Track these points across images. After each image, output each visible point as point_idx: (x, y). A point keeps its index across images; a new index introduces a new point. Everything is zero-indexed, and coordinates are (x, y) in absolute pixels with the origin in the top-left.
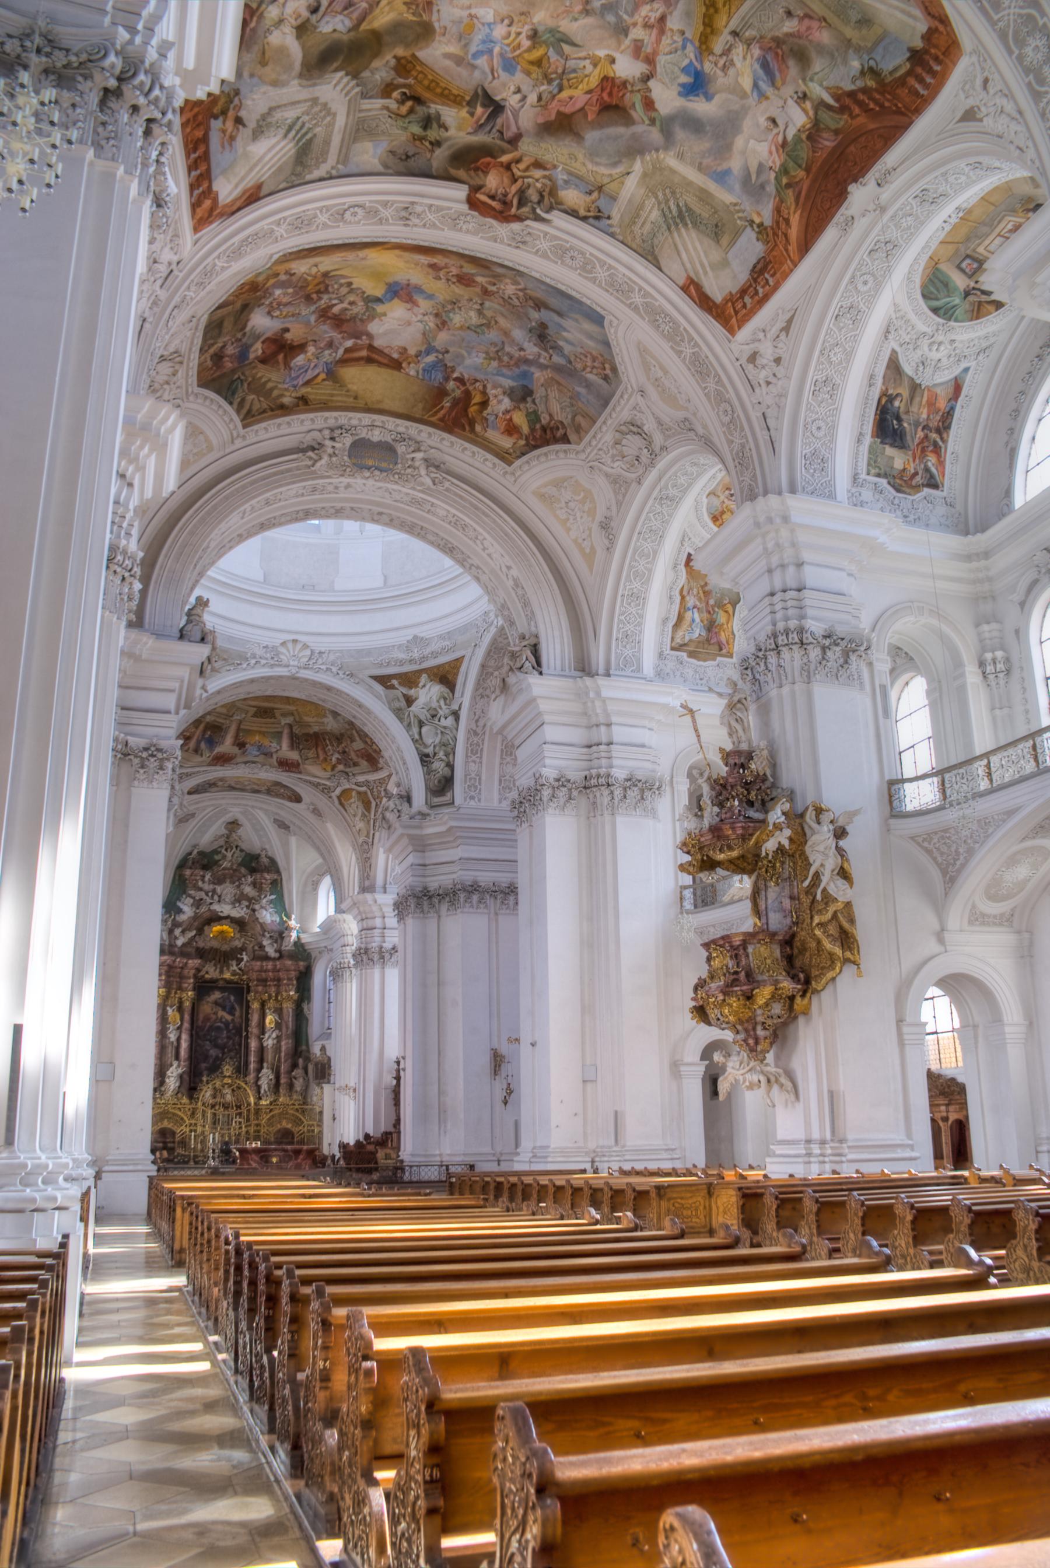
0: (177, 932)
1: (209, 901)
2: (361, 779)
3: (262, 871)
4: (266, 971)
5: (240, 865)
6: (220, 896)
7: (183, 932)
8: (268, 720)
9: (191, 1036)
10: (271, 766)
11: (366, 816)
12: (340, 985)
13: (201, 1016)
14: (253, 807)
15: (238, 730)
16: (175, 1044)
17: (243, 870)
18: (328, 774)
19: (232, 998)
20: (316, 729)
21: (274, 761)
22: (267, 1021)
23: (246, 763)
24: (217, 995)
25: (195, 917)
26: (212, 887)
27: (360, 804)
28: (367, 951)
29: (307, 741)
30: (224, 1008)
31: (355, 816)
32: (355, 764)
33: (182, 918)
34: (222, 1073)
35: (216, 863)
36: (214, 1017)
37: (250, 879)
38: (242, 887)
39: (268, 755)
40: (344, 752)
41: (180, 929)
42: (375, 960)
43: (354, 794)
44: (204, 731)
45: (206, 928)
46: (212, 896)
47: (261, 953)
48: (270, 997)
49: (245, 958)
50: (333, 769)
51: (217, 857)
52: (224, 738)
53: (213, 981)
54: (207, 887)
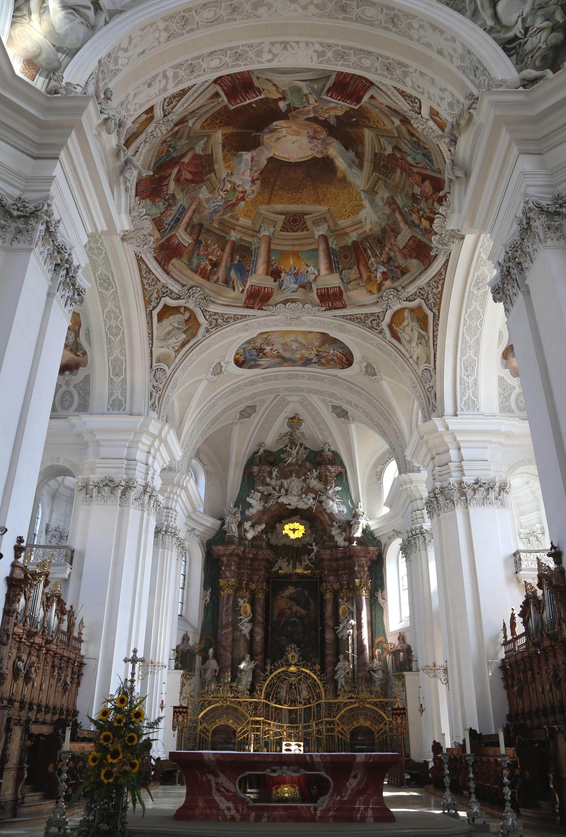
0: (247, 525)
1: (276, 494)
2: (412, 289)
3: (327, 464)
4: (337, 559)
5: (303, 461)
6: (287, 491)
7: (253, 526)
8: (299, 233)
9: (266, 630)
10: (313, 305)
11: (424, 337)
12: (412, 557)
13: (276, 612)
14: (310, 391)
15: (269, 251)
16: (248, 636)
17: (308, 465)
18: (373, 298)
19: (306, 592)
20: (354, 236)
21: (314, 295)
22: (341, 611)
23: (285, 302)
24: (291, 590)
25: (264, 511)
26: (279, 482)
27: (415, 325)
28: (442, 490)
29: (346, 257)
30: (298, 604)
31: (410, 342)
32: (404, 272)
33: (251, 512)
34: (287, 661)
35: (283, 460)
36: (289, 612)
37: (315, 473)
38: (308, 481)
39: (306, 286)
40: (390, 259)
41: (250, 523)
42: (455, 499)
43: (406, 313)
44: (232, 255)
45: (278, 525)
46: (280, 490)
47: (330, 543)
48: (342, 586)
49: (315, 548)
50: (379, 290)
51: (282, 456)
52: (255, 263)
53: (287, 576)
54: (273, 482)
